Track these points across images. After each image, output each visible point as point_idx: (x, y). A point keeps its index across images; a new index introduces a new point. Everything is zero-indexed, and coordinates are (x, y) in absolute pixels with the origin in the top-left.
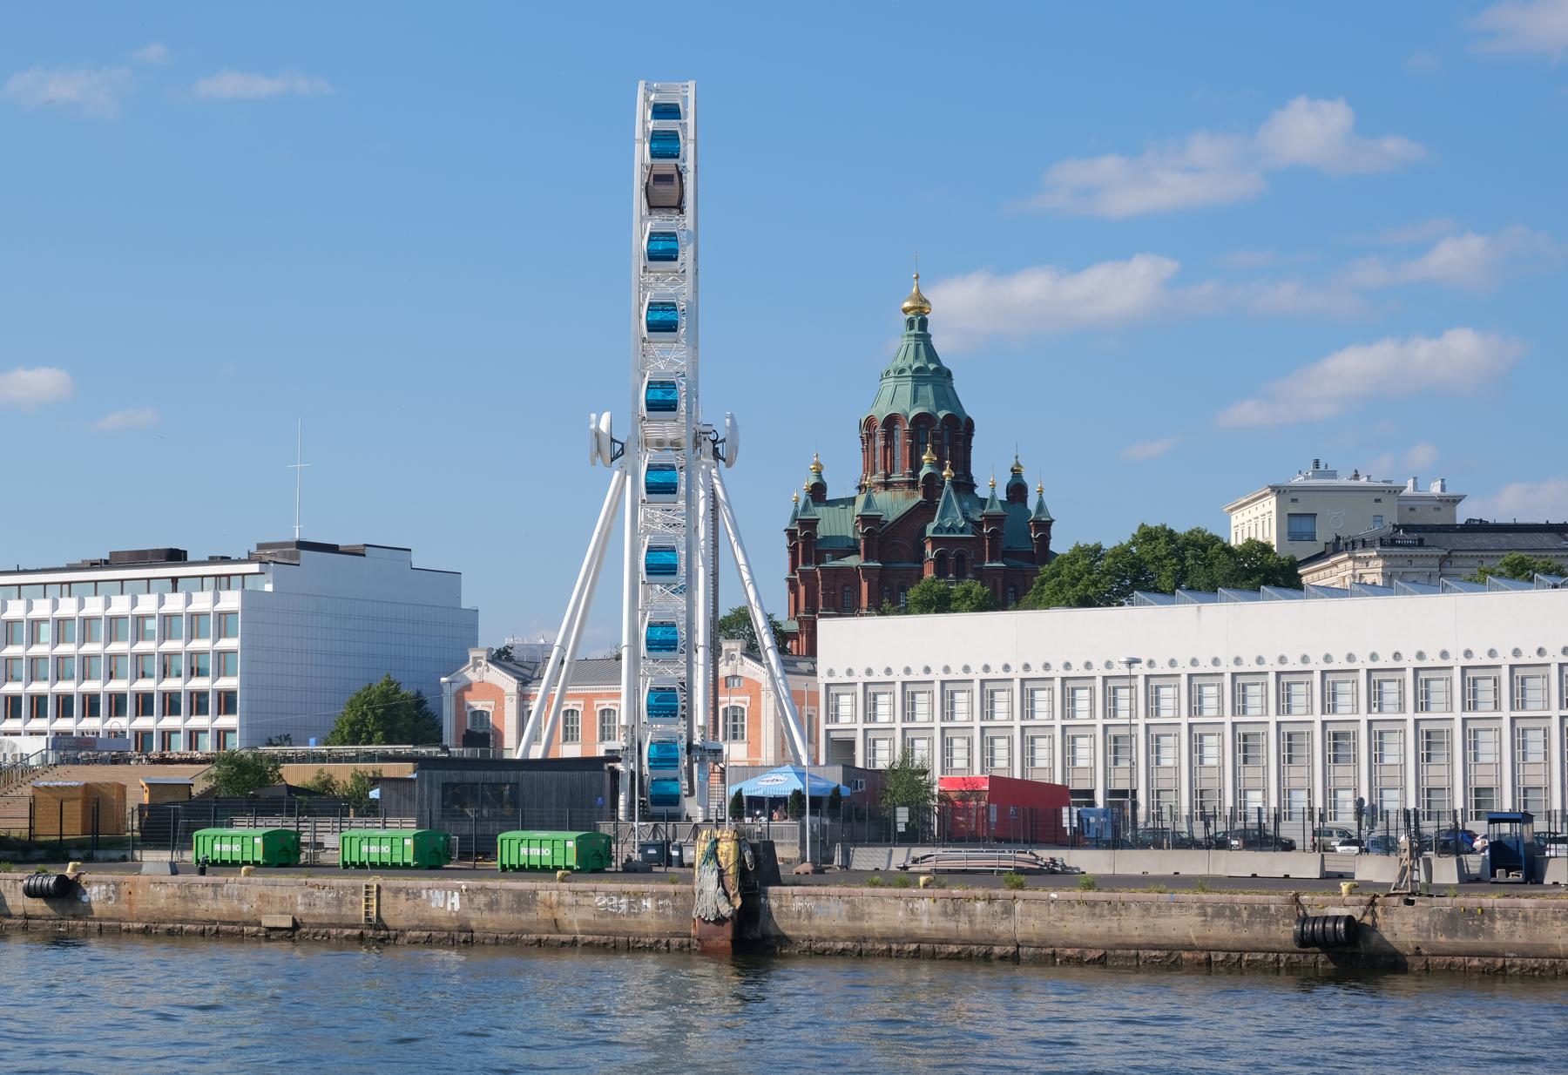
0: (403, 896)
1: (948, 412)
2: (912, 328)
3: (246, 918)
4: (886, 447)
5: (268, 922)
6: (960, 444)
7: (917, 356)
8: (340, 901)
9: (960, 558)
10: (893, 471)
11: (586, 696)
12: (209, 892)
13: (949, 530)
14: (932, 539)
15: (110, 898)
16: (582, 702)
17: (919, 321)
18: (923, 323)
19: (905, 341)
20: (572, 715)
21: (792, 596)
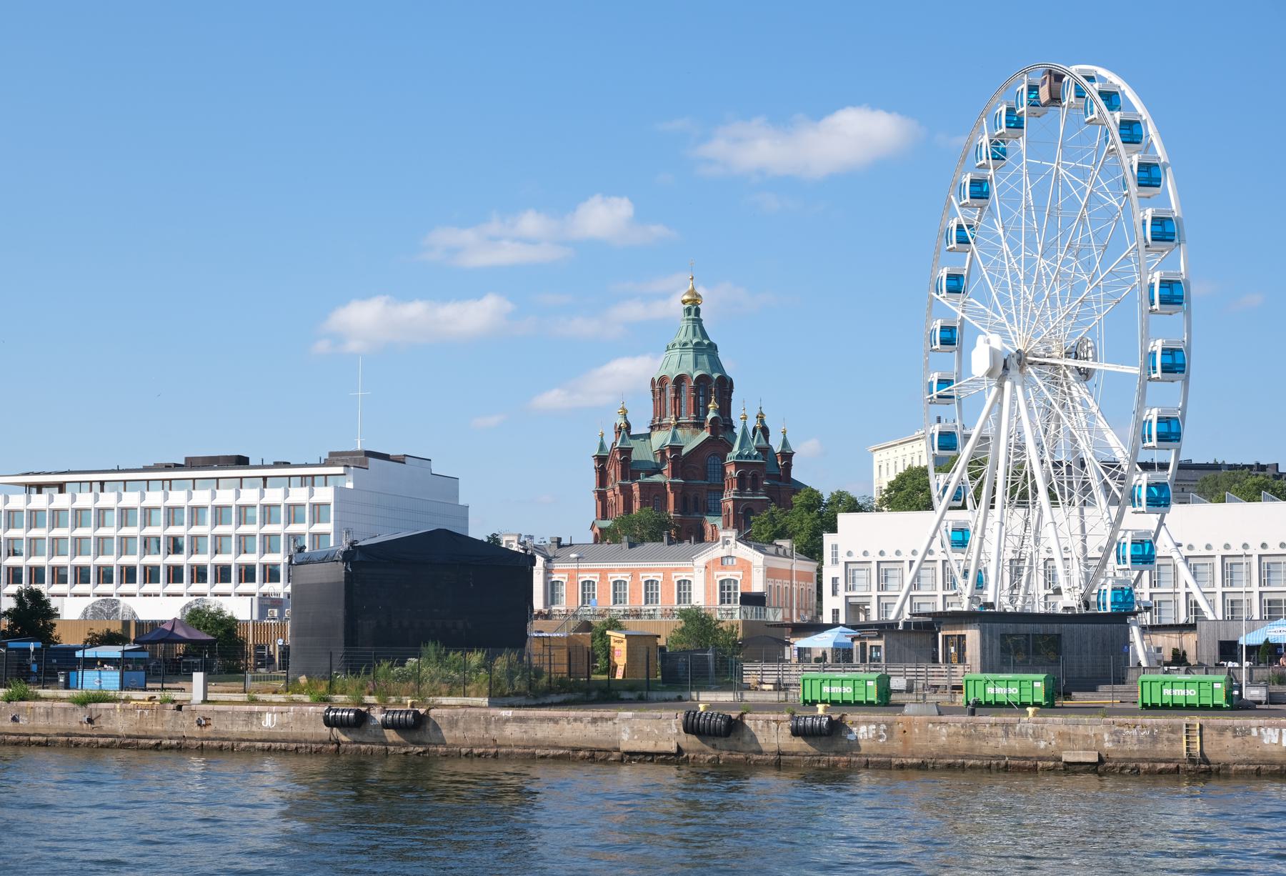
0: (1229, 734)
1: (719, 375)
2: (689, 314)
3: (1042, 754)
4: (675, 398)
5: (1068, 757)
7: (695, 335)
8: (1155, 739)
9: (755, 477)
10: (680, 415)
12: (1000, 731)
13: (749, 456)
15: (880, 737)
16: (598, 575)
17: (693, 308)
18: (698, 311)
19: (684, 324)
20: (589, 584)
21: (600, 503)
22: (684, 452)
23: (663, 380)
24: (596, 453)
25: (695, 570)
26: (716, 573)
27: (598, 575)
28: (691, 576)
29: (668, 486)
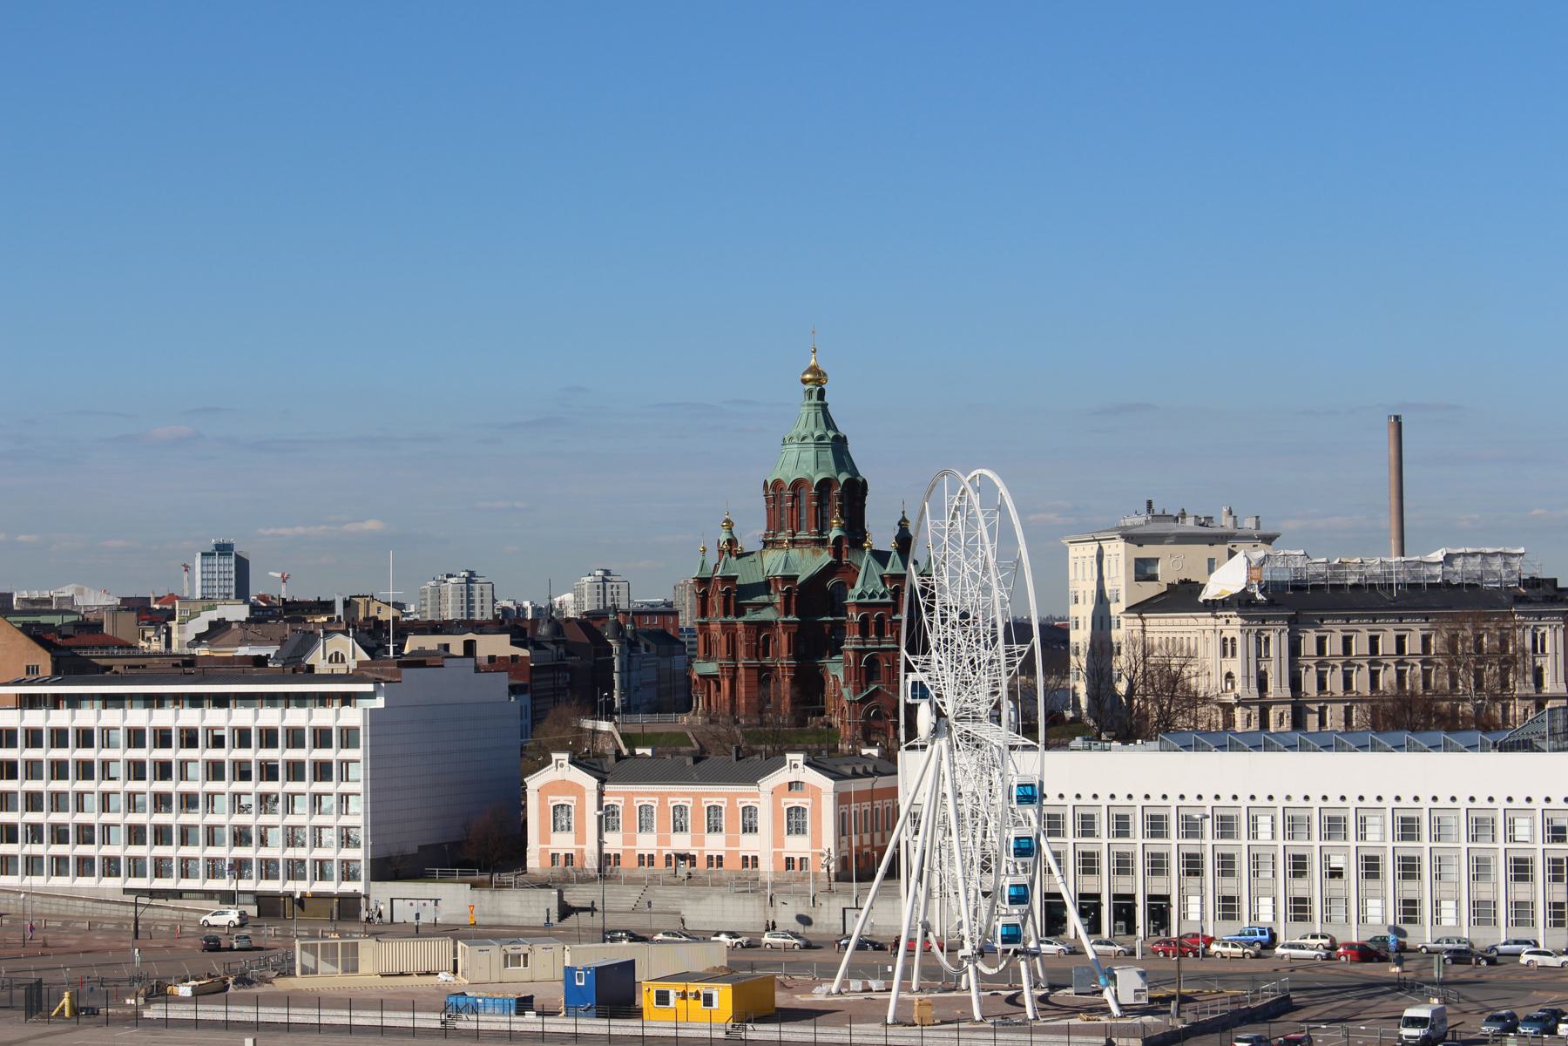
1: (849, 476)
2: (810, 398)
4: (792, 507)
6: (858, 504)
9: (880, 619)
11: (661, 793)
13: (872, 596)
14: (858, 605)
16: (657, 799)
18: (821, 394)
19: (805, 410)
22: (799, 581)
23: (777, 484)
24: (696, 575)
25: (761, 795)
26: (784, 800)
27: (657, 799)
28: (758, 803)
29: (780, 625)
